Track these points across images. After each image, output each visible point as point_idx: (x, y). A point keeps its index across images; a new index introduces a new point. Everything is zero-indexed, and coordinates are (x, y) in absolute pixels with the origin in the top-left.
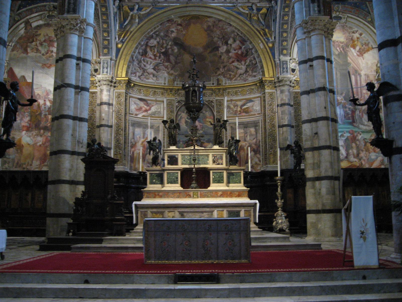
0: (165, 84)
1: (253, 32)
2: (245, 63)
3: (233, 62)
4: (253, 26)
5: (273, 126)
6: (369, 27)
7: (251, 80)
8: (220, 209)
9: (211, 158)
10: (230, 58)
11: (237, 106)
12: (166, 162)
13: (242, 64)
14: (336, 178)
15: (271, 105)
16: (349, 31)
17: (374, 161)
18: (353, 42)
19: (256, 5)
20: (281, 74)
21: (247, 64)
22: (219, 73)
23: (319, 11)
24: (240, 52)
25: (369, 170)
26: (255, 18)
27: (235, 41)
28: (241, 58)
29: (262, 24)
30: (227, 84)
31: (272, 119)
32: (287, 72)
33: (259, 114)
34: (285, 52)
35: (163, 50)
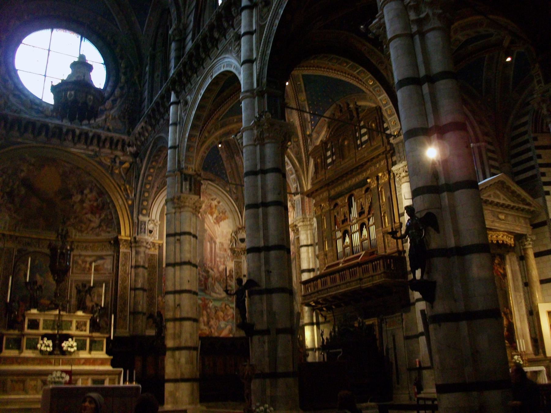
0: (4, 228)
1: (113, 187)
2: (100, 217)
3: (86, 213)
4: (115, 181)
5: (125, 288)
6: (227, 196)
7: (104, 236)
8: (85, 377)
9: (74, 325)
10: (83, 208)
11: (86, 262)
12: (26, 326)
13: (96, 217)
14: (195, 349)
15: (124, 265)
16: (208, 197)
17: (223, 329)
18: (211, 209)
19: (120, 158)
20: (138, 234)
21: (102, 218)
22: (68, 223)
23: (190, 190)
24: (95, 204)
25: (218, 339)
26: (117, 171)
27: (91, 191)
28: (95, 210)
29: (124, 179)
30: (77, 237)
31: (124, 281)
32: (145, 232)
33: (110, 273)
34: (144, 212)
35: (8, 190)
